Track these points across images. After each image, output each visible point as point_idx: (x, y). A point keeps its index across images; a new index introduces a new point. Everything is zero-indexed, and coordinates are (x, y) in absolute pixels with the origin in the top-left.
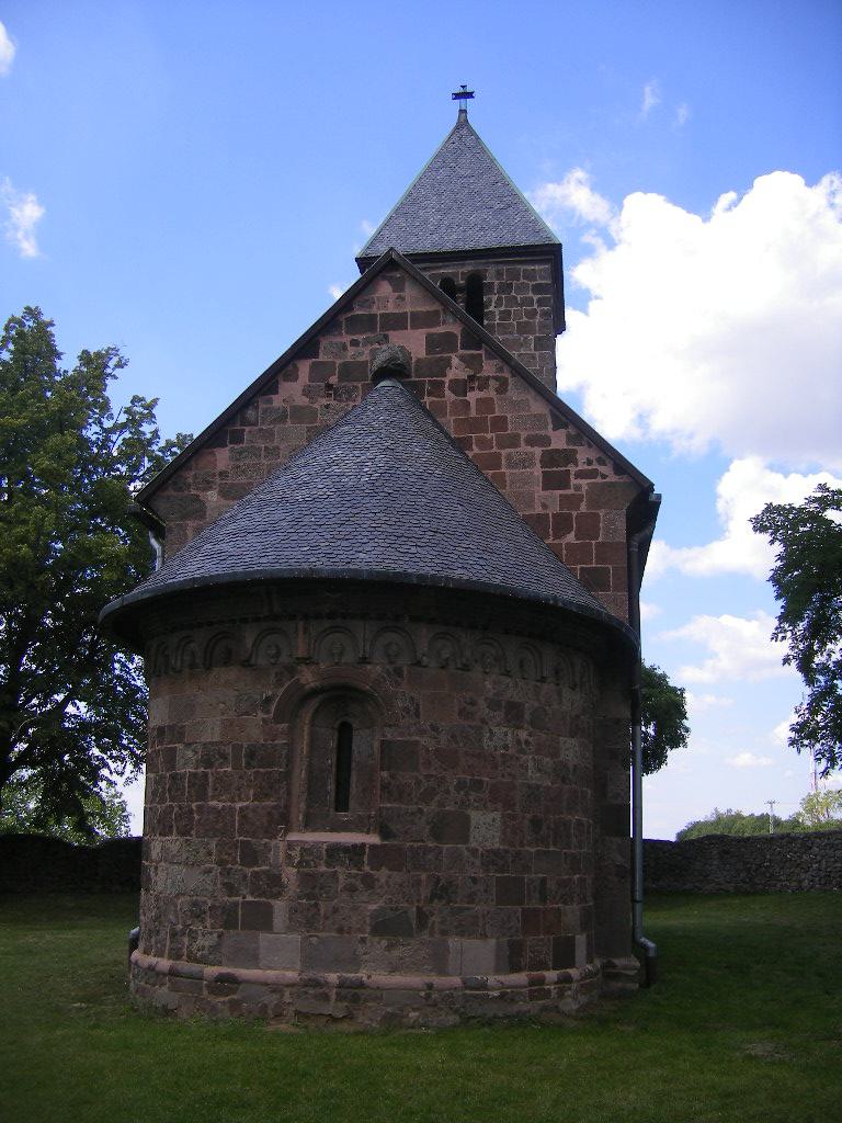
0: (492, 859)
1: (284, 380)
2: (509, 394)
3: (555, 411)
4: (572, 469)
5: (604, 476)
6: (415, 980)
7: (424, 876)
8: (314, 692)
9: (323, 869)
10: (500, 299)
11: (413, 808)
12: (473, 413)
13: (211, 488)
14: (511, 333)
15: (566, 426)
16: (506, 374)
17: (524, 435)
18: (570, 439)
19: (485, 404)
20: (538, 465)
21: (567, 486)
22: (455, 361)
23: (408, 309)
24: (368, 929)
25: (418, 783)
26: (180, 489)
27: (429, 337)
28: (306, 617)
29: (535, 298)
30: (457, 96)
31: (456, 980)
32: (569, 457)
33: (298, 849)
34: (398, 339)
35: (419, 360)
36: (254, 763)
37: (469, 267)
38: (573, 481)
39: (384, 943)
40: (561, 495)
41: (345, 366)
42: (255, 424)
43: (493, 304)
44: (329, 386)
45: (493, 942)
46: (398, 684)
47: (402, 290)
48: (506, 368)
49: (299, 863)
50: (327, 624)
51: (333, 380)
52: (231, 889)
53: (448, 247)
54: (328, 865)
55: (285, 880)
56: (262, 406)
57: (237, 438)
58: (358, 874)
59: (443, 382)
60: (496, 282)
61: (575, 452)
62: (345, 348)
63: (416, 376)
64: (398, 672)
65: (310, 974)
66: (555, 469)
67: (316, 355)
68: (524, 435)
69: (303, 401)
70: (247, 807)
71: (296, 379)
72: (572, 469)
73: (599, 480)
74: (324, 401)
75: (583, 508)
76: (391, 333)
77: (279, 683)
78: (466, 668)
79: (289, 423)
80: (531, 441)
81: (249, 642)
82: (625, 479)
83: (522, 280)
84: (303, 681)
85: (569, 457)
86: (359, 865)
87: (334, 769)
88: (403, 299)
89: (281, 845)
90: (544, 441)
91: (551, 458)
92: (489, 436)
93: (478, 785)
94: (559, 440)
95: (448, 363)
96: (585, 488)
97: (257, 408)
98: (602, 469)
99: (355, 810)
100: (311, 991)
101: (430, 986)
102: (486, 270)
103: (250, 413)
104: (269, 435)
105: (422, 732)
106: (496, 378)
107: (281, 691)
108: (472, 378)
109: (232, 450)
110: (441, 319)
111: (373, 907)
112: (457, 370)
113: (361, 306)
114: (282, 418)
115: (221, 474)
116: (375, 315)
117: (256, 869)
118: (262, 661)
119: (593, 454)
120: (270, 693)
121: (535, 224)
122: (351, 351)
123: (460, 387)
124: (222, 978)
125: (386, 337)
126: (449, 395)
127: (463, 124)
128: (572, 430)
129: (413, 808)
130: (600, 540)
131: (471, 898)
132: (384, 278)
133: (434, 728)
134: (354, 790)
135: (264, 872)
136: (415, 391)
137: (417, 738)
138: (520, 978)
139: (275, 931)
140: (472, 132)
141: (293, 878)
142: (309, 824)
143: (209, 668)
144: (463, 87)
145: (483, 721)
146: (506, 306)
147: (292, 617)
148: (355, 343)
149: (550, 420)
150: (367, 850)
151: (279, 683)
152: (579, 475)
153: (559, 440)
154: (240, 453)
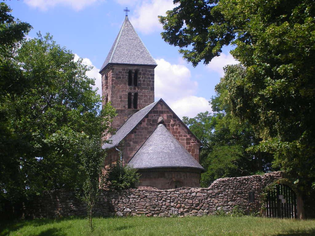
8: (175, 181)
12: (175, 130)
16: (180, 124)
19: (177, 129)
21: (190, 144)
22: (172, 121)
23: (164, 110)
29: (151, 77)
35: (166, 120)
37: (136, 68)
38: (191, 143)
42: (138, 130)
44: (150, 123)
51: (151, 122)
53: (131, 63)
56: (139, 127)
69: (146, 126)
71: (145, 122)
75: (192, 148)
76: (161, 114)
80: (184, 136)
82: (199, 143)
83: (148, 72)
90: (186, 136)
98: (195, 142)
102: (140, 69)
112: (172, 122)
113: (156, 109)
114: (143, 129)
118: (167, 177)
121: (150, 59)
122: (154, 117)
125: (160, 115)
128: (191, 135)
132: (159, 103)
136: (165, 125)
140: (129, 22)
143: (158, 178)
147: (172, 171)
148: (155, 116)
152: (192, 142)
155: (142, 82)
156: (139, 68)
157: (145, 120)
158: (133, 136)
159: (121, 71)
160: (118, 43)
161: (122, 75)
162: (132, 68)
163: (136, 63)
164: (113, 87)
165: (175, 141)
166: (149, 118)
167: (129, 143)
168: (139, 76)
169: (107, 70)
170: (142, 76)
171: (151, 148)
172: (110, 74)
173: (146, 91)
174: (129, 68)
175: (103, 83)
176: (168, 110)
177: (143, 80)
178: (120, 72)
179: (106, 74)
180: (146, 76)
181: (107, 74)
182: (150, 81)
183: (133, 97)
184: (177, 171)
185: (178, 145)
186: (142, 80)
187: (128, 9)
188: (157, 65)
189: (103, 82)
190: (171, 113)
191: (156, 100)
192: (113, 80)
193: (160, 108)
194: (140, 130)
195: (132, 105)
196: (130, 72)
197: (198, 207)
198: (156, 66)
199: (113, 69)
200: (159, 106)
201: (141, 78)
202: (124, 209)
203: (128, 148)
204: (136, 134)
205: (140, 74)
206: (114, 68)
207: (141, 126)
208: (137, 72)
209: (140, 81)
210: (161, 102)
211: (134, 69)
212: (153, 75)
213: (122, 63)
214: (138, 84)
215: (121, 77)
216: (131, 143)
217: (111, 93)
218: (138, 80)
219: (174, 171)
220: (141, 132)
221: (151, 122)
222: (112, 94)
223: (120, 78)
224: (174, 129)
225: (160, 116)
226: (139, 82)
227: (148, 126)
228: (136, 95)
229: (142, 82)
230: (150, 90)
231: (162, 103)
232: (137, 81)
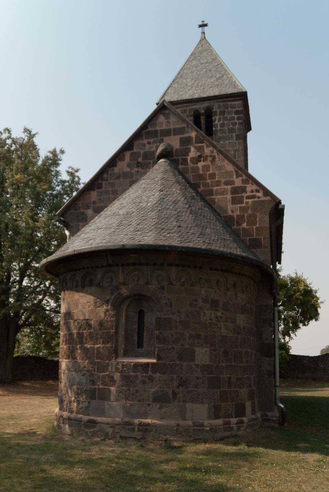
0: (205, 368)
1: (120, 161)
3: (237, 169)
4: (245, 195)
5: (259, 198)
6: (172, 422)
7: (175, 376)
8: (127, 297)
9: (132, 374)
11: (170, 347)
14: (225, 133)
17: (223, 180)
18: (243, 181)
19: (206, 168)
21: (242, 202)
22: (193, 149)
23: (172, 127)
24: (151, 400)
25: (172, 335)
26: (76, 210)
28: (123, 265)
29: (236, 116)
30: (200, 26)
31: (190, 423)
33: (121, 365)
35: (177, 150)
36: (102, 328)
37: (206, 104)
38: (245, 200)
39: (158, 406)
40: (240, 207)
42: (107, 180)
43: (217, 121)
44: (138, 163)
45: (206, 405)
46: (162, 293)
47: (169, 118)
48: (215, 151)
49: (122, 371)
50: (132, 268)
51: (140, 160)
52: (93, 383)
53: (196, 96)
54: (134, 372)
55: (115, 378)
56: (110, 172)
57: (100, 187)
58: (146, 376)
59: (187, 159)
60: (218, 111)
61: (245, 187)
62: (144, 145)
63: (176, 156)
64: (163, 288)
65: (126, 419)
66: (237, 195)
67: (132, 149)
70: (100, 347)
73: (256, 199)
74: (136, 169)
75: (250, 212)
77: (112, 294)
78: (192, 285)
79: (121, 179)
80: (226, 183)
81: (99, 276)
83: (229, 109)
84: (122, 292)
85: (244, 190)
86: (147, 372)
87: (137, 330)
89: (114, 363)
90: (232, 183)
91: (235, 191)
93: (198, 336)
94: (238, 182)
95: (189, 150)
96: (250, 203)
97: (108, 173)
98: (258, 194)
99: (146, 347)
100: (127, 427)
101: (178, 425)
102: (214, 105)
103: (105, 176)
104: (113, 185)
105: (173, 314)
106: (211, 156)
107: (113, 297)
108: (200, 156)
110: (186, 130)
111: (153, 390)
112: (193, 153)
114: (119, 177)
117: (104, 374)
119: (255, 187)
120: (108, 298)
121: (234, 84)
122: (147, 147)
124: (90, 421)
127: (203, 39)
128: (244, 177)
129: (170, 347)
130: (258, 225)
131: (196, 386)
132: (161, 113)
133: (179, 312)
134: (145, 339)
135: (107, 375)
137: (171, 316)
138: (220, 422)
139: (112, 400)
141: (118, 377)
142: (126, 354)
144: (203, 21)
145: (201, 308)
146: (223, 121)
147: (117, 265)
148: (149, 143)
149: (234, 174)
150: (150, 365)
151: (112, 294)
152: (248, 197)
154: (101, 193)
155: (219, 128)
156: (211, 104)
157: (124, 155)
162: (198, 106)
167: (83, 213)
170: (217, 118)
173: (227, 142)
174: (194, 107)
177: (221, 124)
180: (226, 115)
187: (205, 23)
194: (110, 180)
204: (103, 189)
207: (113, 170)
208: (209, 114)
211: (203, 108)
213: (179, 99)
219: (123, 265)
220: (113, 185)
225: (162, 141)
227: (131, 169)
229: (219, 128)
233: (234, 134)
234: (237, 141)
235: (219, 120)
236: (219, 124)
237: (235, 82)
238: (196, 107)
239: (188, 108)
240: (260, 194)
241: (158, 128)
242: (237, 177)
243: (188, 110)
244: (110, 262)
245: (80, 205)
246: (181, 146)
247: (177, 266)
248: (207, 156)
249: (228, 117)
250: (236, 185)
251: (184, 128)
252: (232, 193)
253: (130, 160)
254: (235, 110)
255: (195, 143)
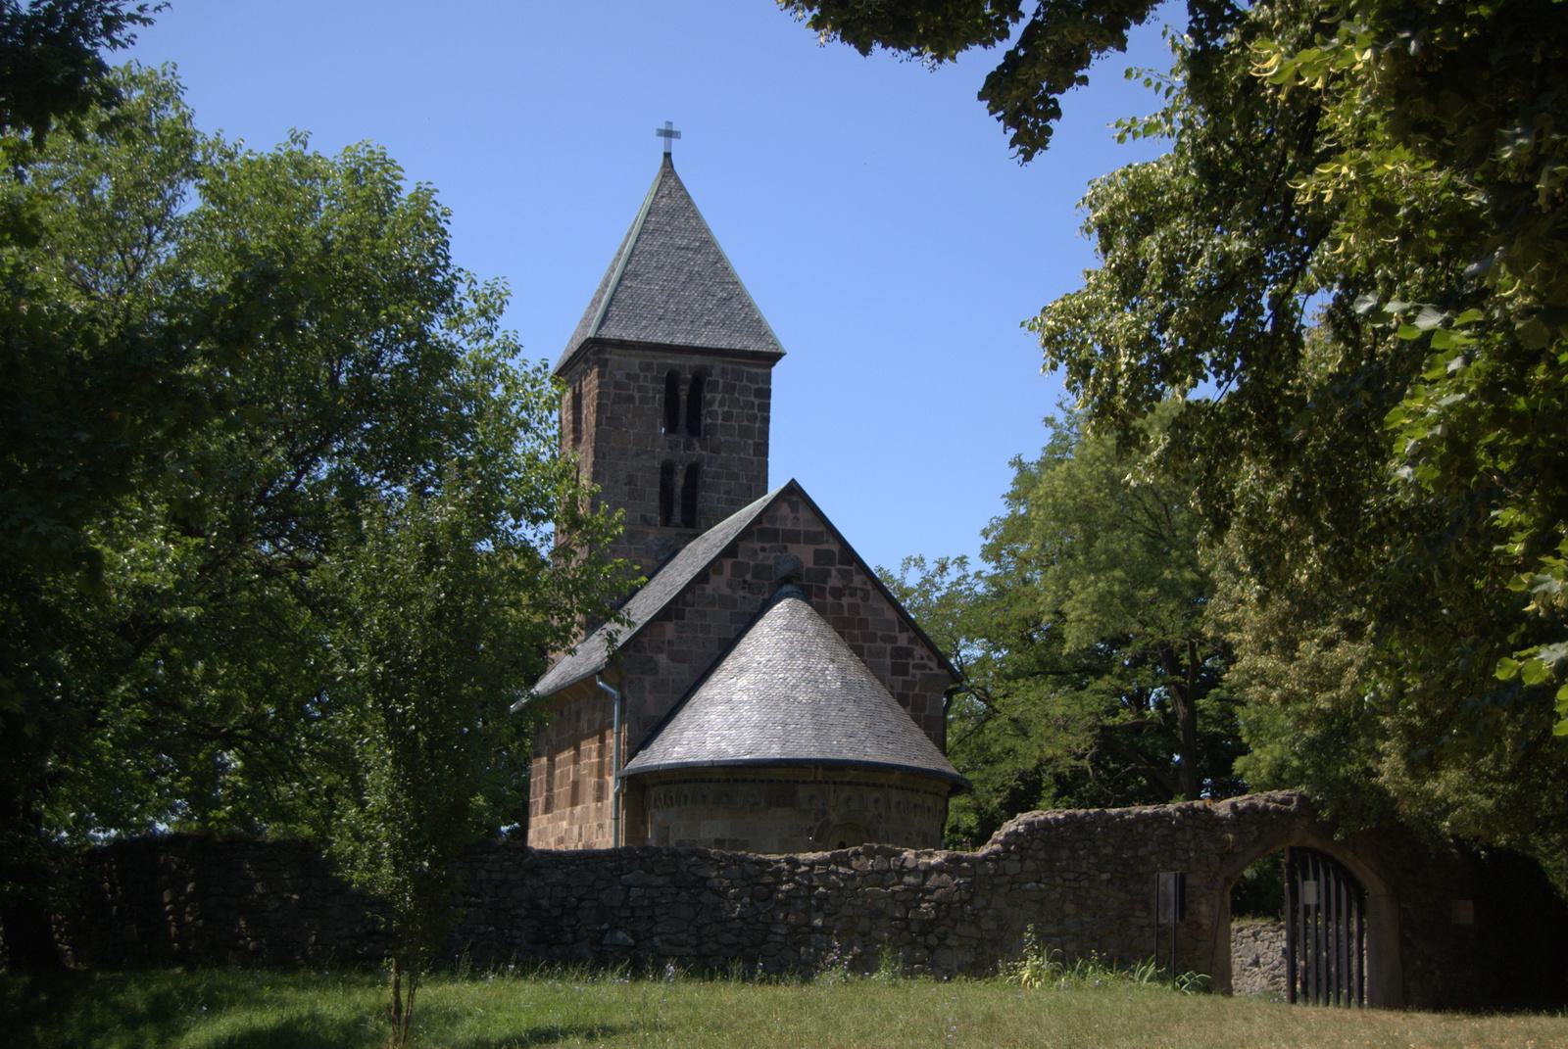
2: (870, 602)
4: (911, 662)
5: (931, 669)
10: (723, 398)
12: (846, 614)
13: (661, 652)
15: (908, 631)
16: (869, 587)
17: (880, 634)
18: (910, 641)
19: (854, 608)
20: (889, 657)
21: (905, 672)
22: (834, 573)
23: (802, 528)
26: (639, 651)
27: (816, 551)
32: (909, 653)
34: (794, 550)
35: (808, 569)
37: (697, 361)
38: (911, 670)
41: (756, 566)
42: (693, 606)
43: (717, 403)
44: (745, 582)
47: (797, 512)
48: (869, 583)
51: (748, 577)
56: (698, 592)
57: (680, 615)
61: (913, 649)
64: (880, 815)
67: (736, 557)
68: (880, 634)
69: (727, 591)
72: (911, 662)
74: (741, 593)
75: (917, 690)
76: (789, 545)
80: (885, 639)
82: (945, 672)
83: (745, 382)
85: (909, 653)
88: (798, 519)
90: (894, 640)
92: (856, 632)
94: (903, 640)
96: (918, 676)
102: (712, 367)
103: (689, 597)
107: (818, 824)
108: (845, 587)
109: (676, 624)
112: (835, 581)
115: (669, 642)
116: (778, 530)
119: (925, 652)
121: (757, 327)
122: (761, 555)
123: (838, 593)
125: (785, 548)
126: (829, 599)
128: (912, 634)
130: (927, 712)
140: (678, 180)
144: (670, 123)
147: (827, 782)
148: (763, 549)
151: (817, 819)
152: (916, 666)
153: (903, 640)
155: (720, 422)
157: (721, 565)
158: (670, 629)
159: (638, 371)
160: (628, 263)
161: (640, 389)
162: (678, 362)
163: (697, 343)
164: (600, 438)
165: (844, 654)
166: (740, 559)
167: (651, 659)
168: (709, 396)
169: (581, 366)
170: (718, 397)
171: (742, 682)
172: (591, 384)
174: (670, 361)
175: (564, 422)
176: (821, 528)
178: (628, 376)
179: (577, 384)
180: (736, 395)
181: (580, 386)
182: (752, 418)
183: (679, 481)
184: (849, 783)
185: (856, 672)
186: (720, 412)
187: (675, 129)
188: (784, 354)
189: (564, 417)
190: (831, 539)
191: (775, 486)
192: (600, 408)
193: (786, 519)
195: (677, 511)
196: (672, 381)
197: (932, 940)
198: (775, 357)
199: (603, 364)
200: (785, 509)
201: (716, 404)
202: (603, 933)
203: (648, 679)
204: (686, 621)
205: (714, 386)
206: (607, 360)
207: (703, 589)
208: (699, 381)
209: (713, 414)
210: (793, 490)
211: (690, 367)
212: (765, 394)
214: (702, 428)
215: (637, 395)
216: (663, 659)
217: (591, 460)
218: (704, 412)
219: (835, 783)
221: (748, 577)
222: (594, 465)
223: (630, 399)
224: (841, 606)
226: (709, 421)
228: (693, 472)
229: (720, 422)
230: (751, 452)
231: (795, 498)
232: (700, 415)
233: (751, 442)
234: (755, 458)
235: (722, 404)
236: (720, 411)
237: (759, 321)
238: (673, 361)
239: (655, 362)
240: (933, 664)
241: (779, 526)
242: (900, 632)
243: (655, 367)
244: (820, 778)
245: (646, 645)
246: (815, 563)
247: (897, 788)
248: (856, 589)
249: (741, 399)
250: (899, 644)
251: (821, 533)
252: (892, 656)
253: (733, 575)
254: (756, 386)
255: (841, 563)
